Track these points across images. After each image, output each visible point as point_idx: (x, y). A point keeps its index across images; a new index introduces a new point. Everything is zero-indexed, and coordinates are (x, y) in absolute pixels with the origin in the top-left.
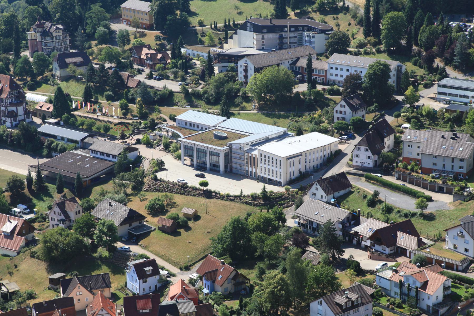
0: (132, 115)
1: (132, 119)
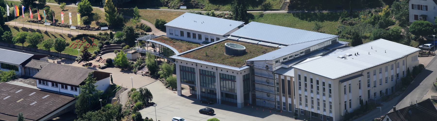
0: (98, 24)
1: (98, 29)
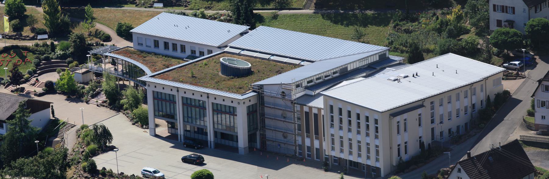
0: (33, 30)
1: (33, 39)
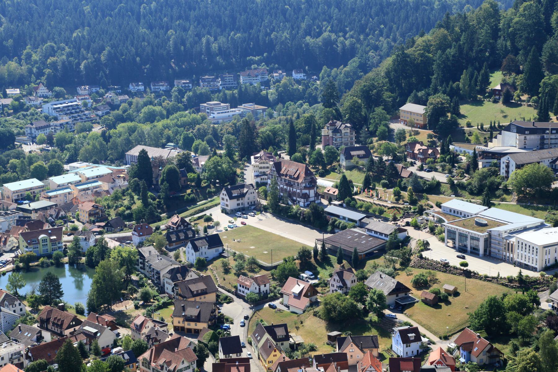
0: (403, 201)
1: (403, 204)
